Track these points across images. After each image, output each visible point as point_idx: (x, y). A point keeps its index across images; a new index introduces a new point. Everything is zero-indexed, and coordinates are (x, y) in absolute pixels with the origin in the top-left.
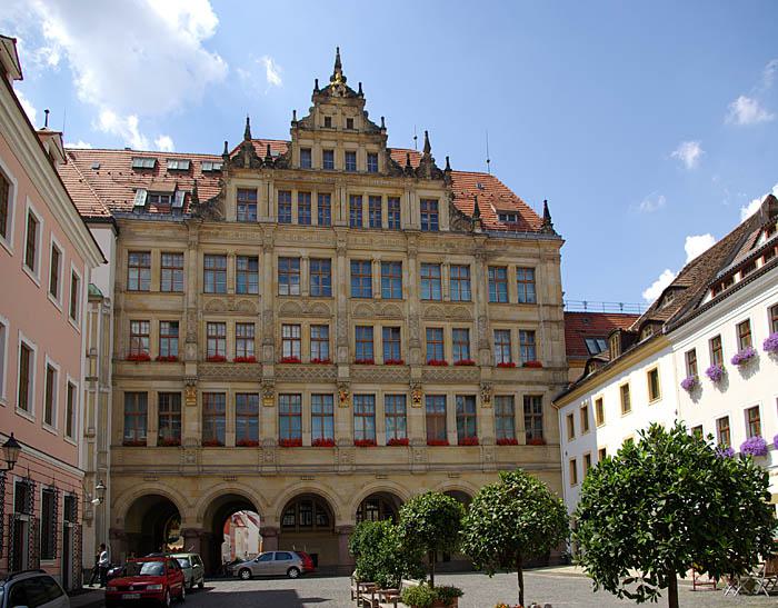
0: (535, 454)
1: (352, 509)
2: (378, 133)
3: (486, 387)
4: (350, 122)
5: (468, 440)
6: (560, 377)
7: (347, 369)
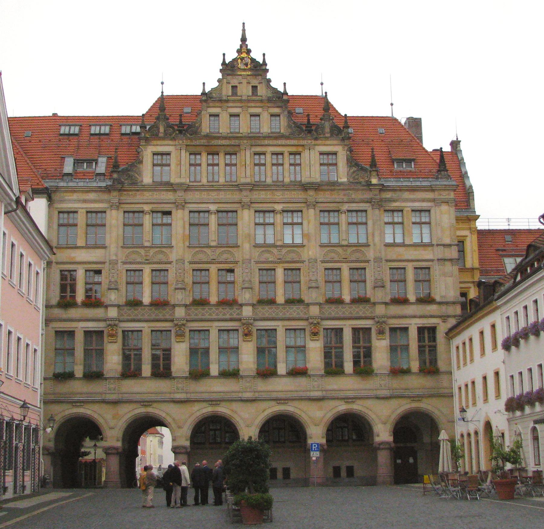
3: (380, 322)
4: (255, 88)
7: (250, 308)
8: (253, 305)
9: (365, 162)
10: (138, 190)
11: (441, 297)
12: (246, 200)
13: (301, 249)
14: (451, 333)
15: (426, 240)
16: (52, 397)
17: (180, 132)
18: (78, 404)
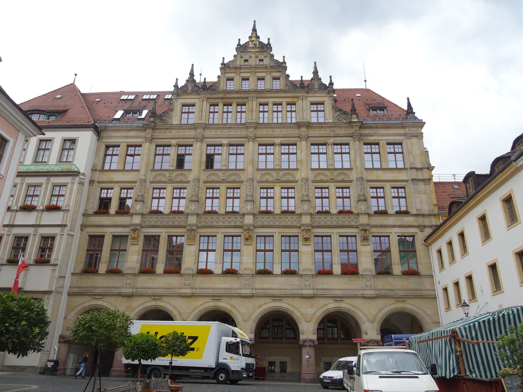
0: (411, 282)
1: (252, 325)
2: (282, 66)
5: (350, 270)
6: (427, 221)
7: (251, 217)
8: (254, 215)
9: (348, 108)
10: (167, 129)
11: (417, 210)
12: (252, 135)
13: (295, 172)
14: (428, 240)
15: (400, 165)
16: (76, 290)
17: (204, 89)
18: (97, 297)
